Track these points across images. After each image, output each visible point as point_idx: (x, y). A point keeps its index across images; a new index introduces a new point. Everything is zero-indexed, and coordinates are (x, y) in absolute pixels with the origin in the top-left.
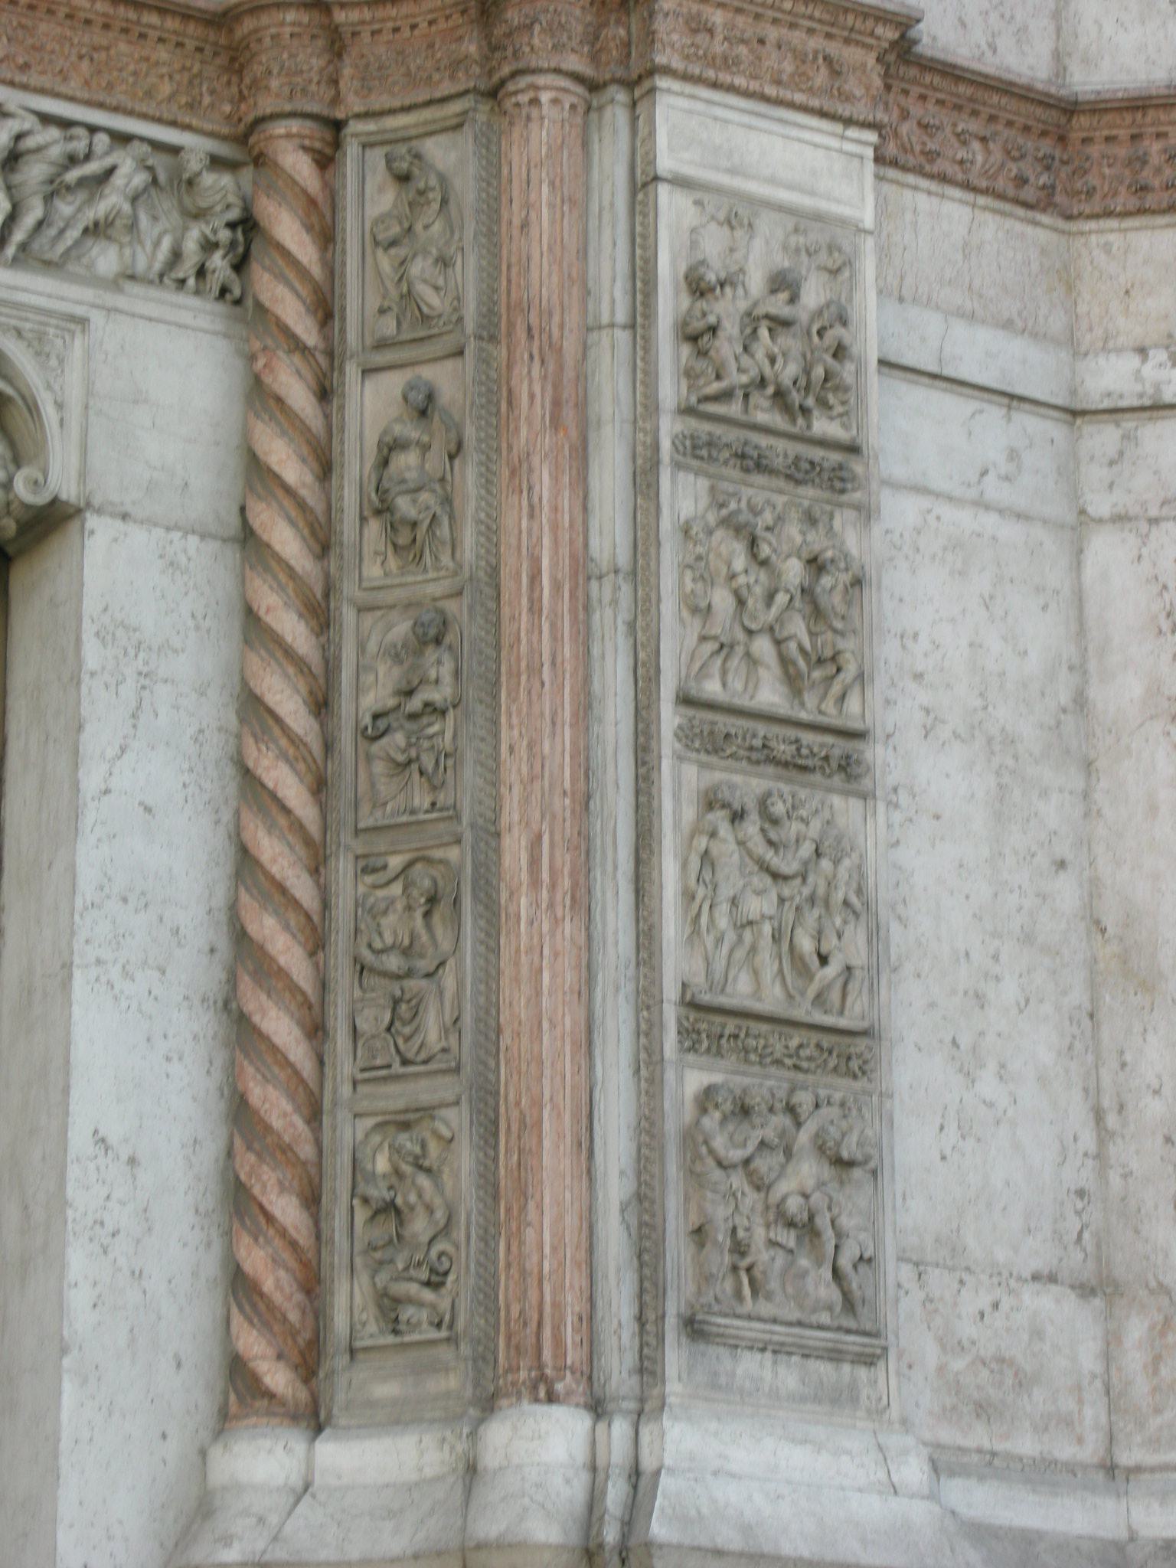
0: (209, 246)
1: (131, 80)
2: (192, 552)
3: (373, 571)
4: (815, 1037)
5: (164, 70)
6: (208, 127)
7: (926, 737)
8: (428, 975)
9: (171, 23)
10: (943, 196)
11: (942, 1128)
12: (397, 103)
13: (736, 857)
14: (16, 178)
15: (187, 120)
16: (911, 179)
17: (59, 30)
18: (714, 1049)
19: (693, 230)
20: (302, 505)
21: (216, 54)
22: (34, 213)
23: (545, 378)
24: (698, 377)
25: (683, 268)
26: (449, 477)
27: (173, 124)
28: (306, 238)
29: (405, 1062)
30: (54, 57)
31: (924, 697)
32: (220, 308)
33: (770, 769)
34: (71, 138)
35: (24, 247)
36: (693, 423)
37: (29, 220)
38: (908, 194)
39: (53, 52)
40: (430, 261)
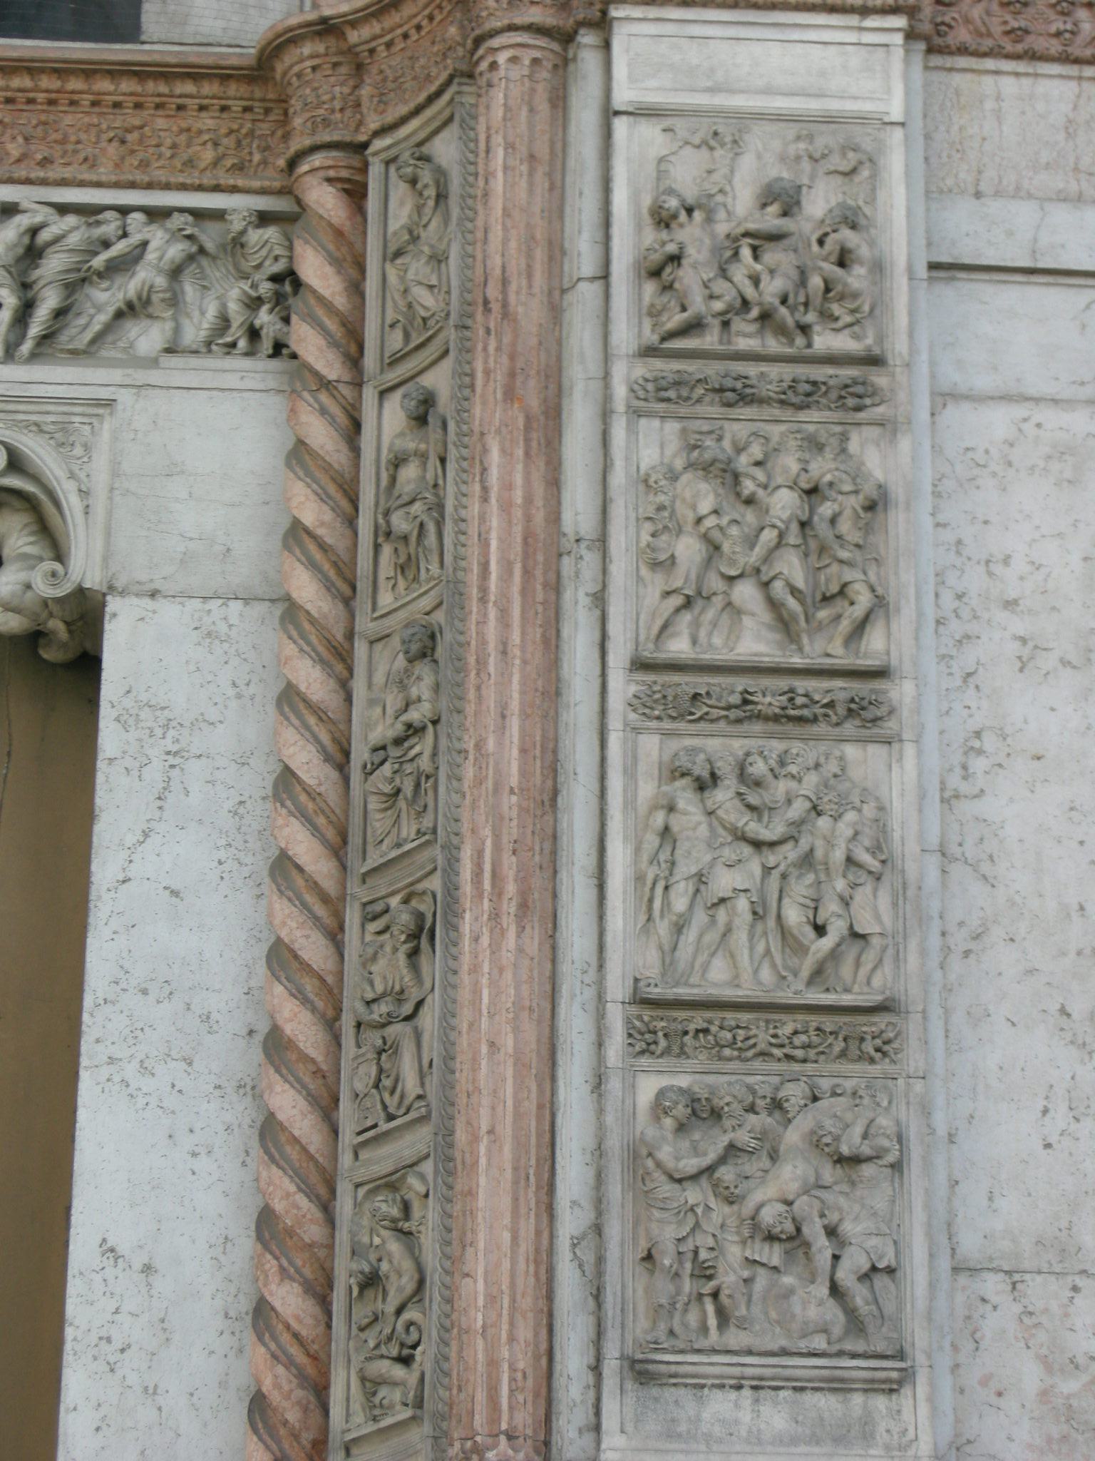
0: (254, 303)
1: (168, 153)
2: (234, 620)
3: (386, 599)
4: (814, 1020)
5: (206, 137)
6: (256, 184)
7: (1021, 670)
8: (408, 1018)
9: (209, 88)
10: (1036, 75)
11: (1045, 1111)
12: (404, 110)
13: (703, 830)
14: (35, 274)
15: (231, 182)
16: (990, 64)
17: (86, 120)
18: (676, 1049)
19: (661, 160)
20: (323, 547)
21: (267, 111)
22: (49, 301)
23: (498, 349)
24: (660, 313)
25: (647, 201)
26: (441, 482)
27: (217, 189)
28: (329, 270)
29: (391, 1118)
30: (80, 146)
31: (1019, 626)
32: (275, 364)
33: (758, 727)
34: (98, 223)
35: (47, 338)
36: (658, 364)
37: (43, 312)
38: (988, 80)
39: (78, 142)
40: (423, 260)
